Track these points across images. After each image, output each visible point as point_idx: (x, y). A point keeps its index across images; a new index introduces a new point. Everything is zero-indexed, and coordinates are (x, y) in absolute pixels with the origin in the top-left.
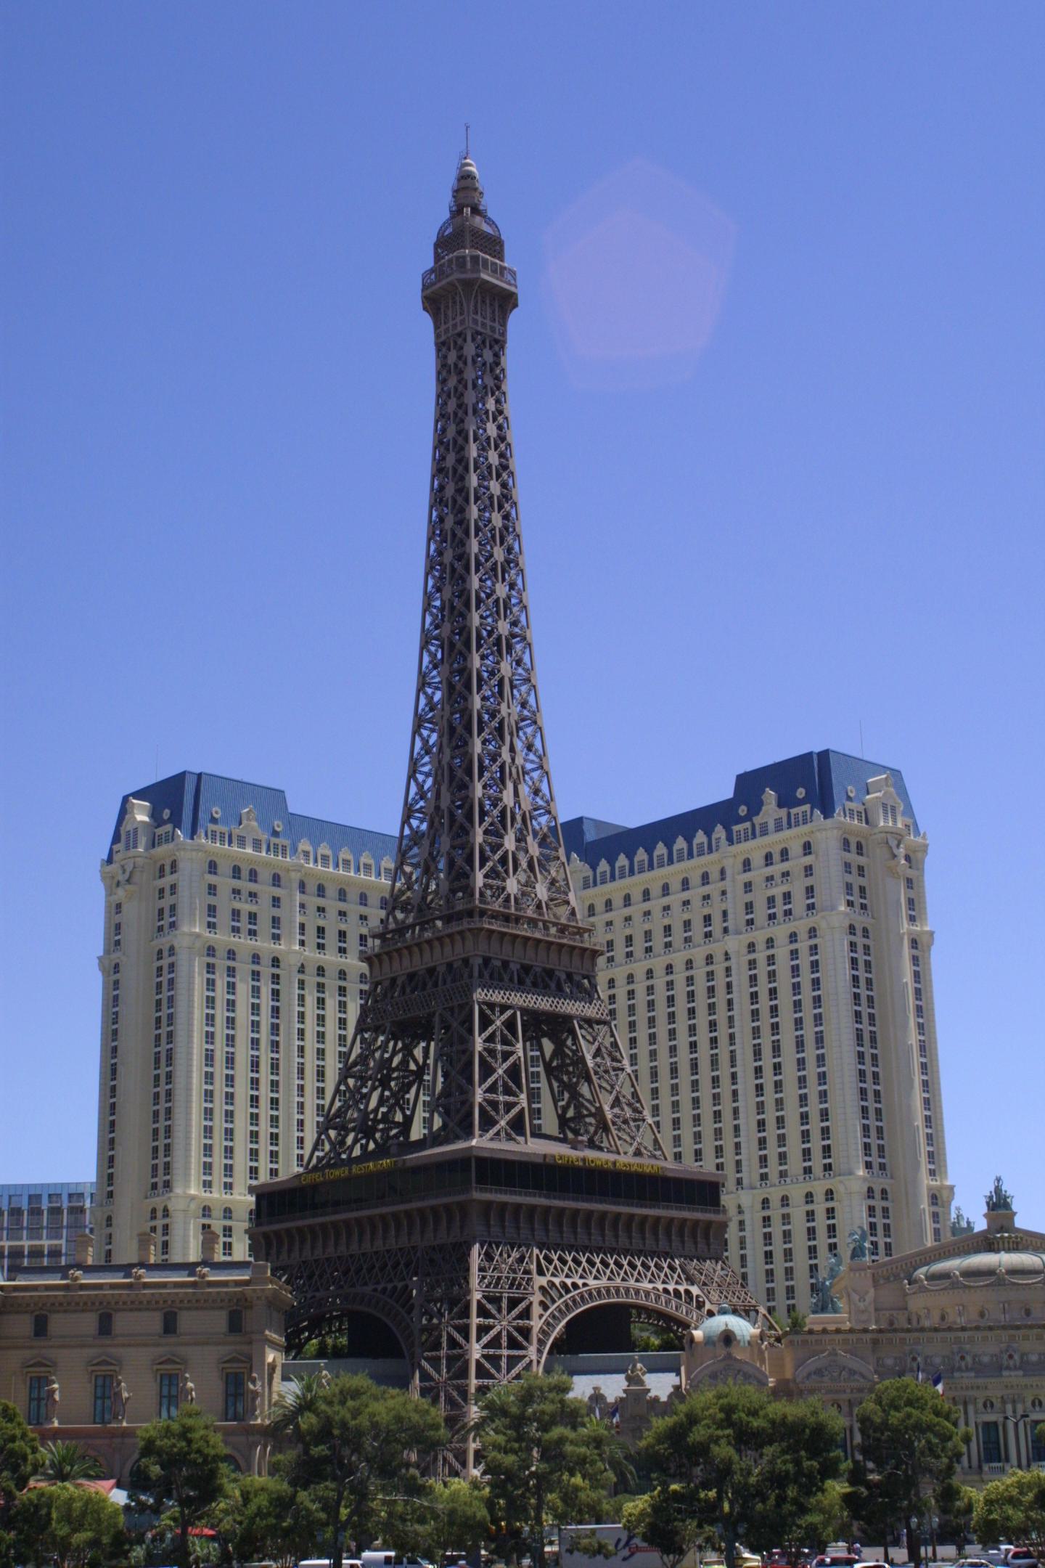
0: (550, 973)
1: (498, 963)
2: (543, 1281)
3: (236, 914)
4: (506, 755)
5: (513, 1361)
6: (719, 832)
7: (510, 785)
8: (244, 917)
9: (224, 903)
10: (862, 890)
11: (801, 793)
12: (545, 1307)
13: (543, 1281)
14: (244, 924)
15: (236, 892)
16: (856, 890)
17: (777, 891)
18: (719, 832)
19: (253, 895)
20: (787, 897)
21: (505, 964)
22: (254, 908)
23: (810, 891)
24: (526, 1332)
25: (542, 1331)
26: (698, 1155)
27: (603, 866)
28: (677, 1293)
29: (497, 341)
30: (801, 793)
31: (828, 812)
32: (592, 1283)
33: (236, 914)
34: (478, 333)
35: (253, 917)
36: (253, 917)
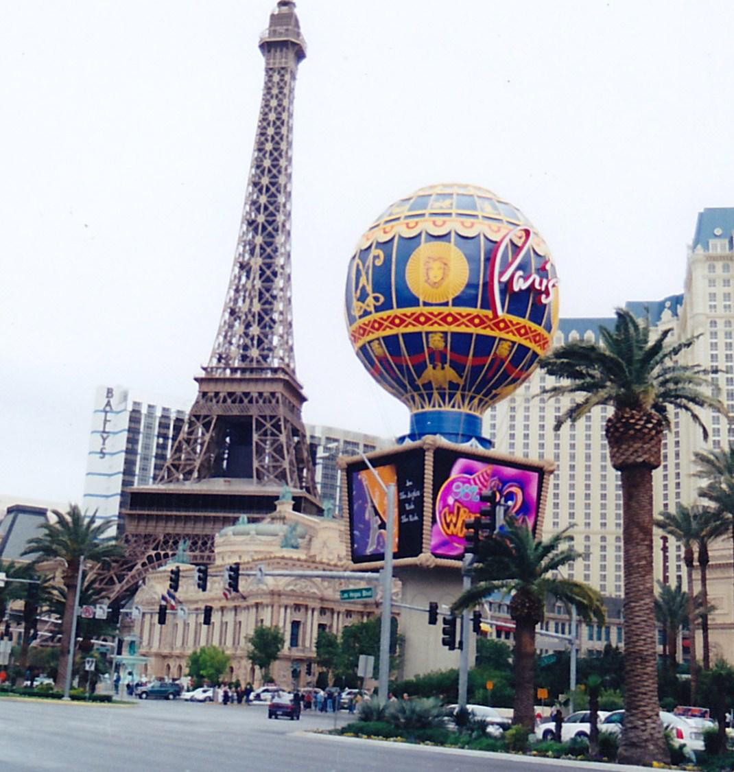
0: (246, 394)
1: (213, 394)
2: (153, 553)
12: (144, 565)
21: (217, 394)
29: (283, 68)
34: (271, 69)
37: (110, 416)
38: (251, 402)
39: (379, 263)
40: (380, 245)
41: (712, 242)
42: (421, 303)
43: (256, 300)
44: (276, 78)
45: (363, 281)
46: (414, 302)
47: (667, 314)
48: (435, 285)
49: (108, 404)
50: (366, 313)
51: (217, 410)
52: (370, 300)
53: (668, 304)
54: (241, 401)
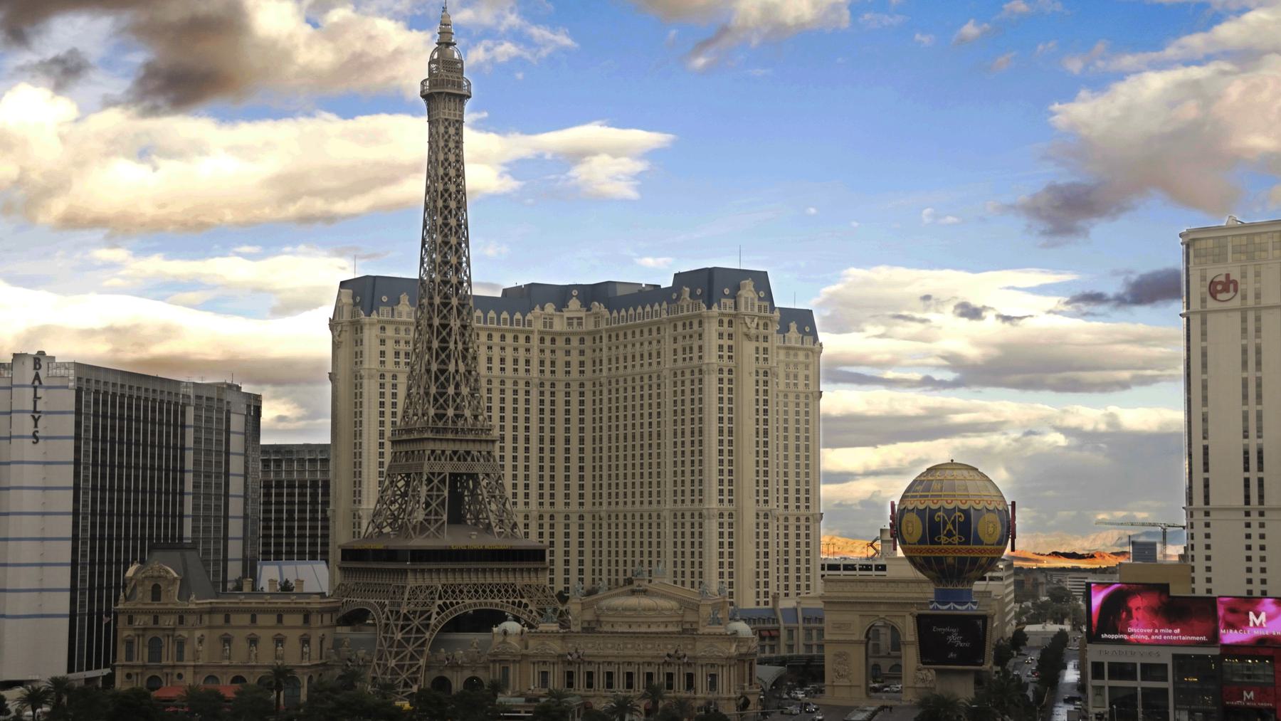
0: (468, 453)
2: (441, 602)
4: (452, 346)
5: (417, 639)
6: (665, 305)
7: (453, 361)
10: (730, 348)
12: (438, 614)
13: (441, 602)
16: (726, 348)
18: (665, 305)
21: (443, 452)
23: (700, 348)
24: (428, 625)
25: (436, 626)
26: (541, 535)
27: (615, 314)
28: (514, 603)
30: (699, 292)
32: (467, 601)
37: (40, 392)
38: (473, 460)
39: (962, 520)
40: (960, 510)
41: (723, 300)
43: (460, 362)
44: (452, 131)
45: (949, 526)
46: (981, 543)
47: (574, 304)
48: (990, 535)
49: (37, 377)
50: (950, 543)
51: (448, 469)
52: (956, 539)
53: (575, 293)
54: (465, 460)
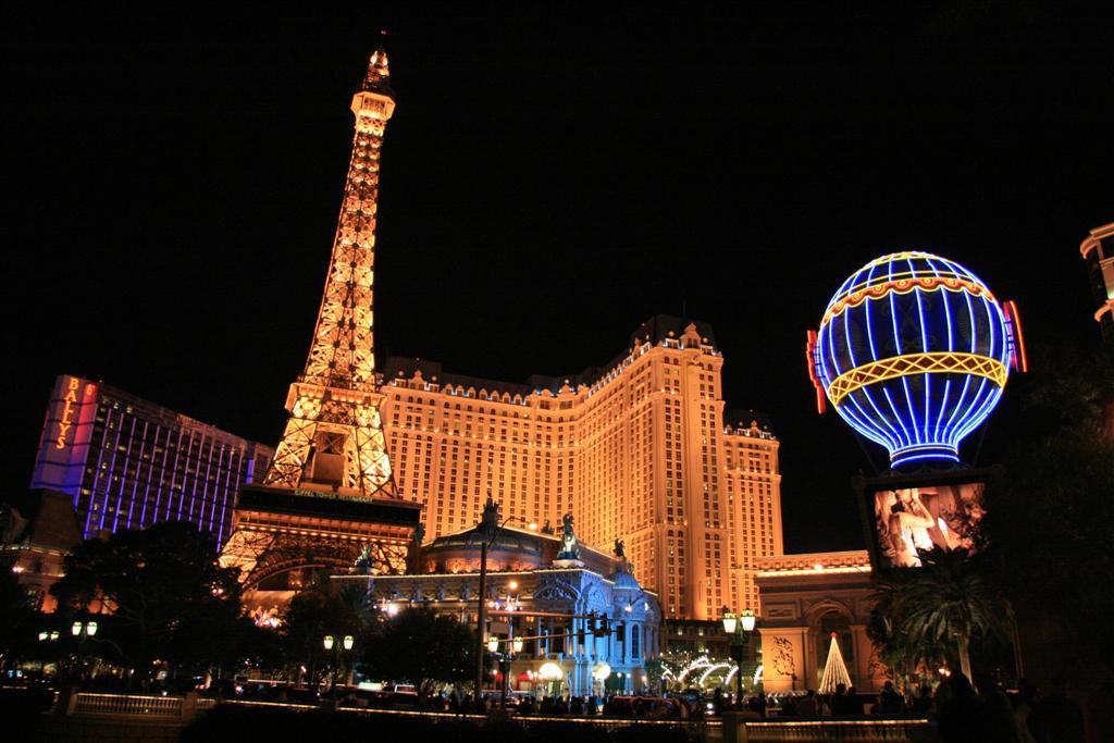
3: (409, 418)
8: (414, 419)
9: (404, 414)
10: (676, 382)
11: (648, 337)
14: (413, 422)
15: (410, 408)
17: (639, 387)
19: (420, 409)
20: (643, 388)
22: (418, 415)
30: (648, 337)
31: (654, 344)
33: (409, 418)
35: (418, 419)
36: (418, 419)
42: (973, 350)
